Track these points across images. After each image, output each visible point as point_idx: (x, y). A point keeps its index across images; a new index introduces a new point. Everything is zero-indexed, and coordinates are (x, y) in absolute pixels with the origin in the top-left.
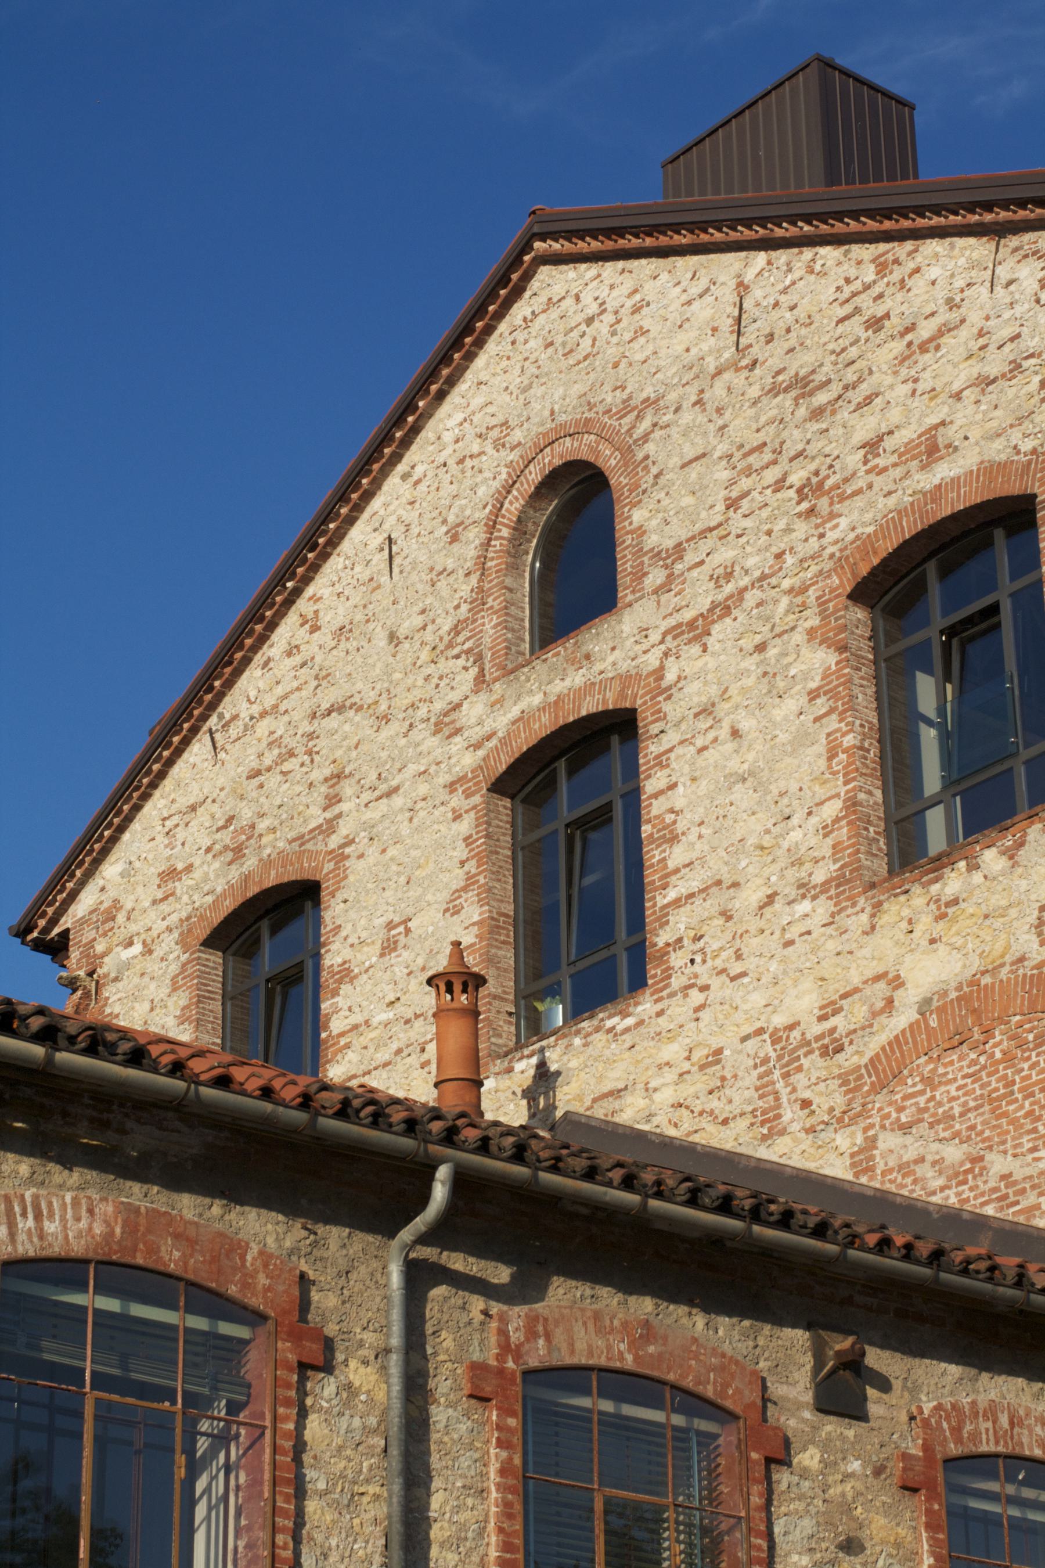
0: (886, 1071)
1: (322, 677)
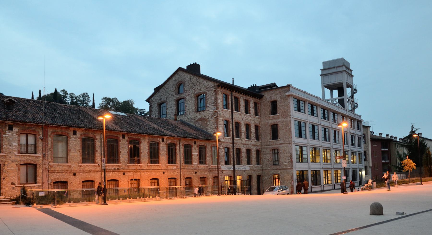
0: (197, 121)
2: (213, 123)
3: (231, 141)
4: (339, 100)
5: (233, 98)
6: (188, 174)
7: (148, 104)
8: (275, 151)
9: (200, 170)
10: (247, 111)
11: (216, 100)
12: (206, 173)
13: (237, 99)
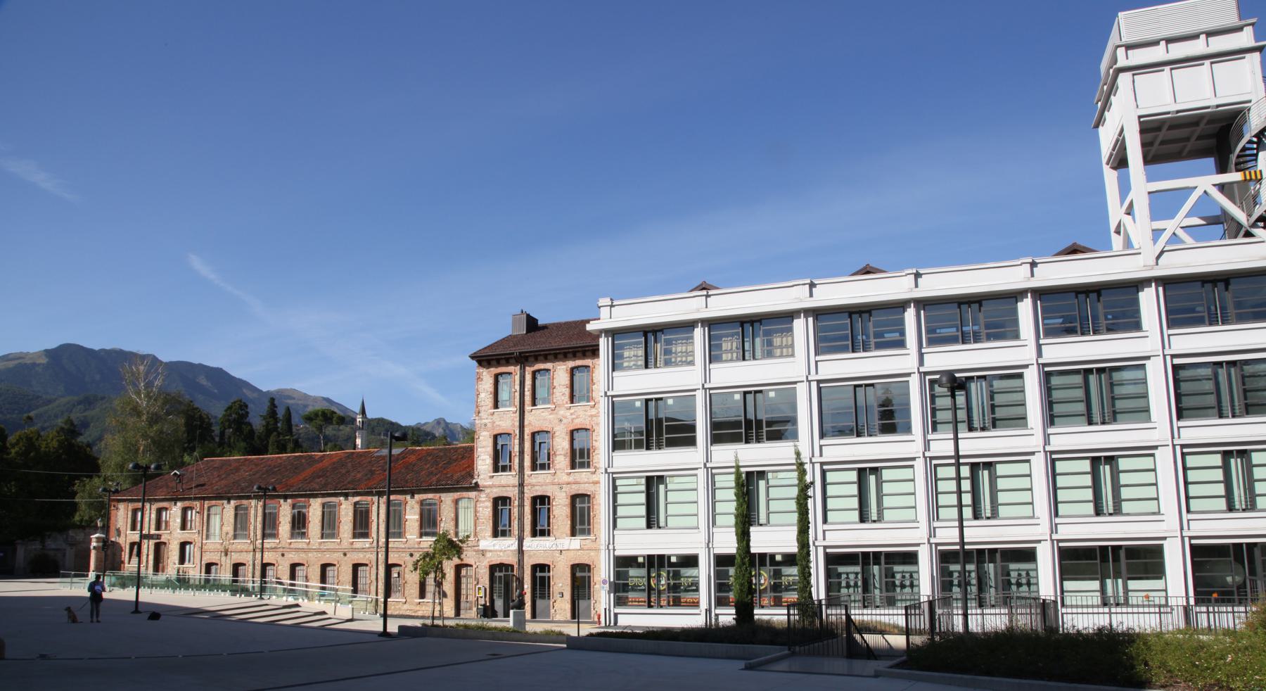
3: (515, 481)
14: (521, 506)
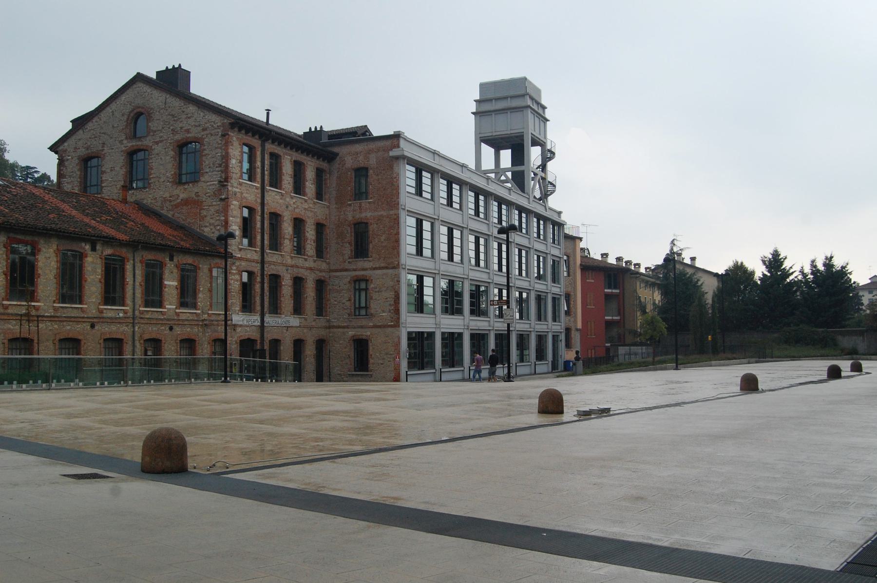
0: (177, 206)
1: (102, 128)
2: (217, 212)
3: (257, 257)
4: (514, 174)
5: (267, 157)
6: (152, 331)
7: (54, 158)
8: (360, 284)
9: (182, 323)
10: (299, 188)
11: (226, 158)
12: (196, 330)
13: (275, 158)
14: (262, 283)
